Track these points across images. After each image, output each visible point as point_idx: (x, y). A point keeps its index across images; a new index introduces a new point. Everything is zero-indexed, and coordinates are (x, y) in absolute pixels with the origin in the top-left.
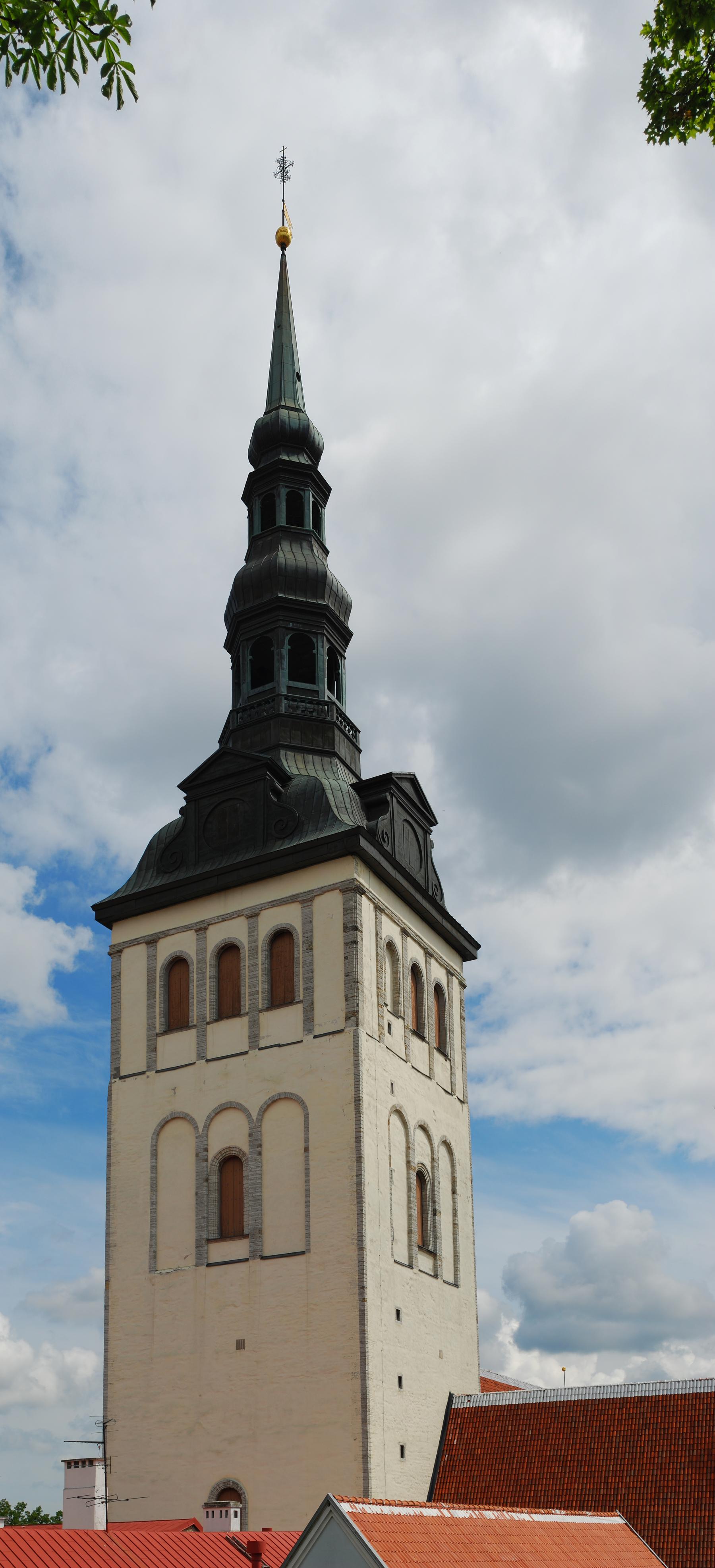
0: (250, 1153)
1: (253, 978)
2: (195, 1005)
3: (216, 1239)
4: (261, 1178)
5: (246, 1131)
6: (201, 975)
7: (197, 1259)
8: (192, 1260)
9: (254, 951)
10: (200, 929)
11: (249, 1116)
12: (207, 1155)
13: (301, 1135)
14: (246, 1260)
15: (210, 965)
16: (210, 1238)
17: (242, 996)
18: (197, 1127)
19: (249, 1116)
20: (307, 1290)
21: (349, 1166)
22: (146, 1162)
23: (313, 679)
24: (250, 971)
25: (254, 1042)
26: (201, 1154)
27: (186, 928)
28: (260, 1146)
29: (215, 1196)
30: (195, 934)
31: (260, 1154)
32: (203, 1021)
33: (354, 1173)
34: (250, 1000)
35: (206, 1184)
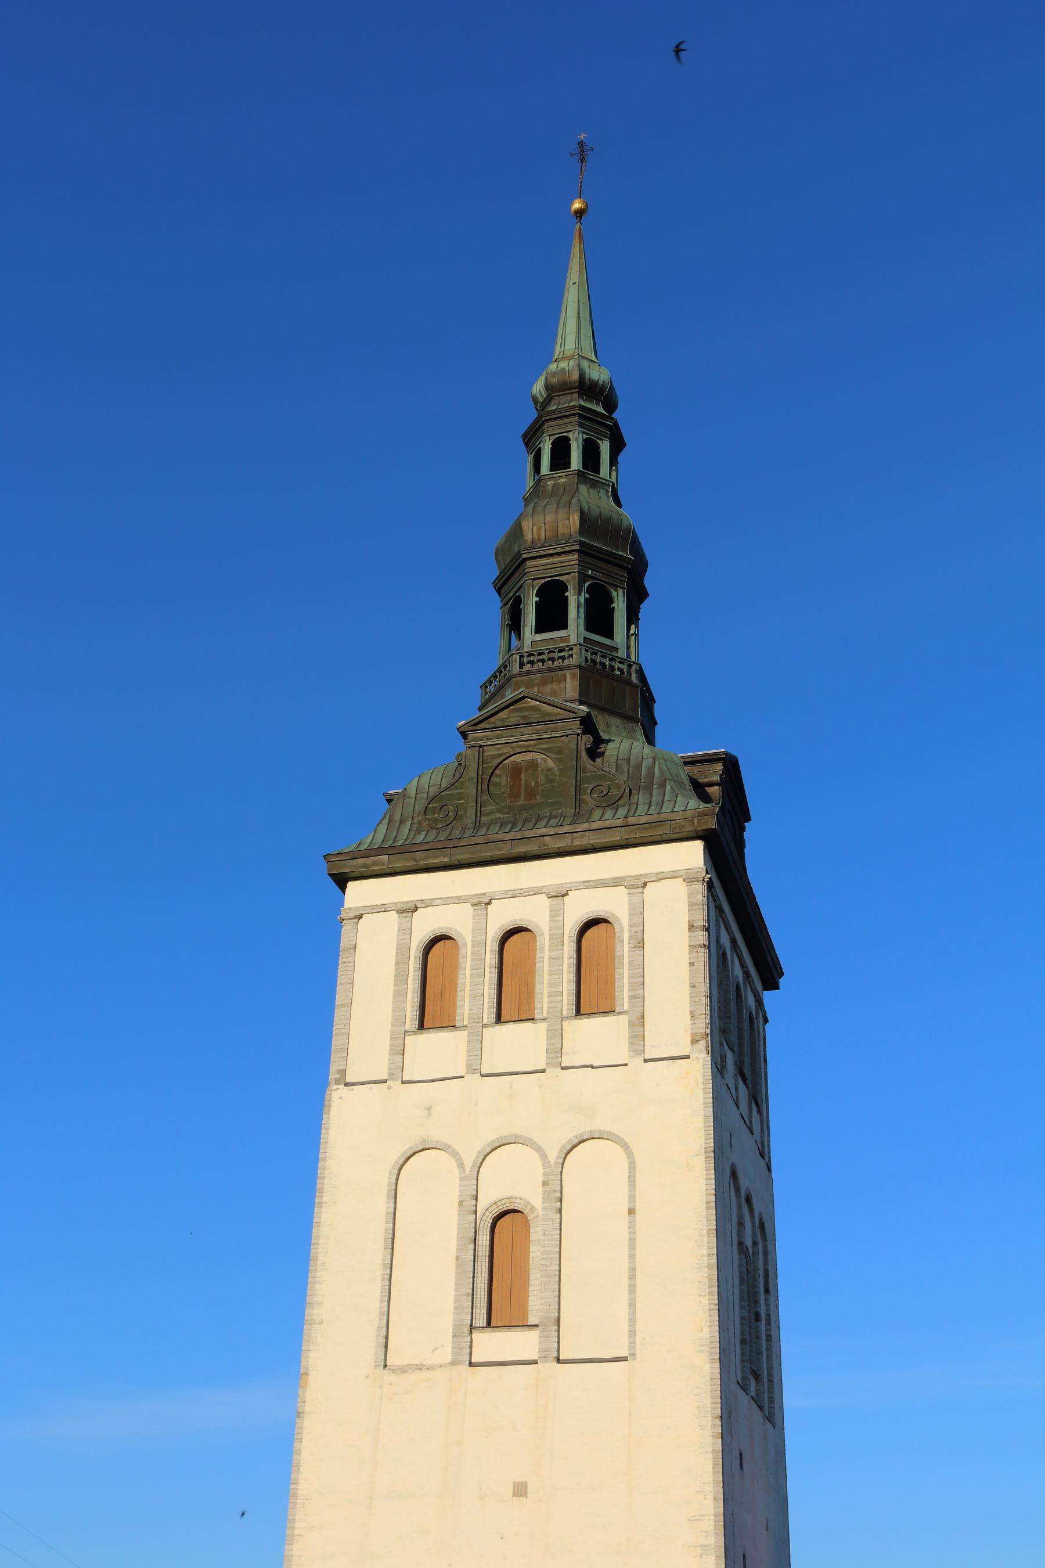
0: (544, 1209)
1: (554, 974)
2: (467, 1000)
3: (483, 1327)
5: (540, 1179)
7: (453, 1354)
8: (447, 1355)
11: (543, 1156)
14: (535, 1362)
15: (491, 951)
19: (543, 1156)
22: (381, 1205)
23: (611, 636)
27: (460, 900)
30: (472, 909)
31: (560, 1211)
32: (478, 1023)
34: (549, 1002)
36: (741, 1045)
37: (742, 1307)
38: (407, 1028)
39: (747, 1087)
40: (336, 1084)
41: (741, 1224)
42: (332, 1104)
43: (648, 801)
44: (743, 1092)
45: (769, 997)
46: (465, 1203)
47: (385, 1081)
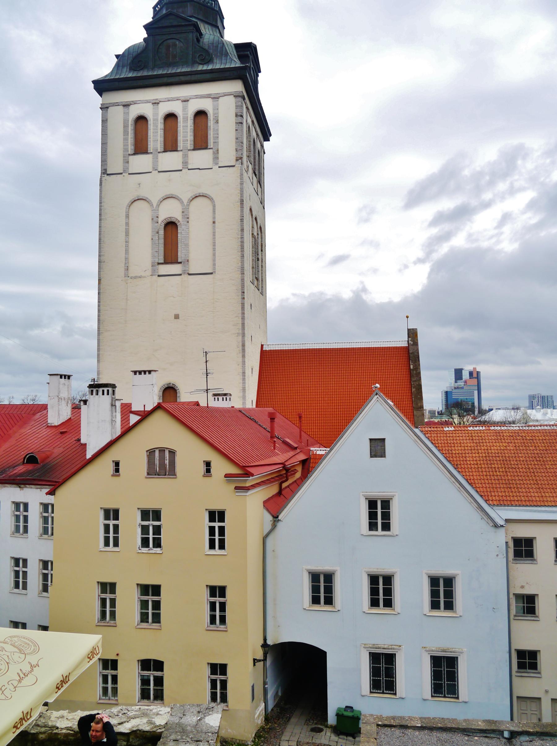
4: (188, 234)
5: (181, 211)
6: (156, 127)
7: (152, 272)
8: (149, 273)
9: (186, 119)
10: (155, 103)
12: (158, 220)
13: (211, 214)
14: (180, 275)
15: (161, 122)
16: (159, 262)
17: (178, 141)
18: (152, 205)
20: (214, 292)
21: (237, 233)
22: (123, 220)
24: (183, 129)
25: (185, 165)
26: (155, 220)
27: (147, 102)
28: (188, 218)
29: (162, 241)
31: (188, 222)
33: (240, 237)
35: (157, 235)
36: (255, 162)
37: (253, 256)
38: (130, 153)
39: (257, 178)
40: (104, 174)
41: (253, 227)
42: (103, 182)
43: (220, 62)
44: (255, 180)
45: (266, 144)
46: (154, 219)
47: (121, 174)
